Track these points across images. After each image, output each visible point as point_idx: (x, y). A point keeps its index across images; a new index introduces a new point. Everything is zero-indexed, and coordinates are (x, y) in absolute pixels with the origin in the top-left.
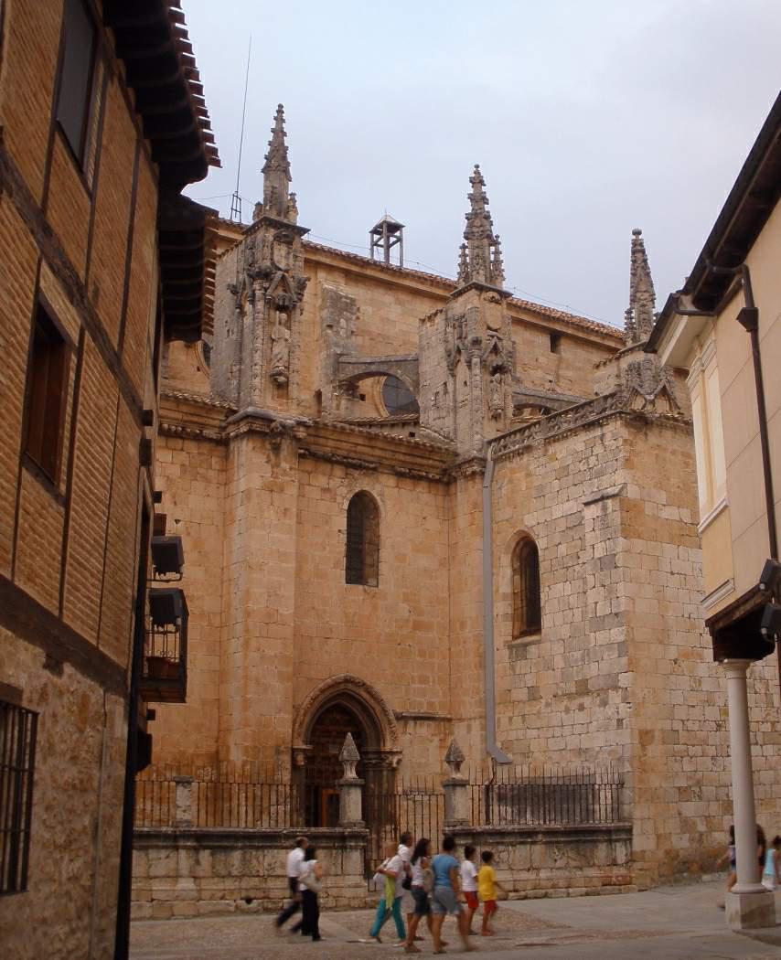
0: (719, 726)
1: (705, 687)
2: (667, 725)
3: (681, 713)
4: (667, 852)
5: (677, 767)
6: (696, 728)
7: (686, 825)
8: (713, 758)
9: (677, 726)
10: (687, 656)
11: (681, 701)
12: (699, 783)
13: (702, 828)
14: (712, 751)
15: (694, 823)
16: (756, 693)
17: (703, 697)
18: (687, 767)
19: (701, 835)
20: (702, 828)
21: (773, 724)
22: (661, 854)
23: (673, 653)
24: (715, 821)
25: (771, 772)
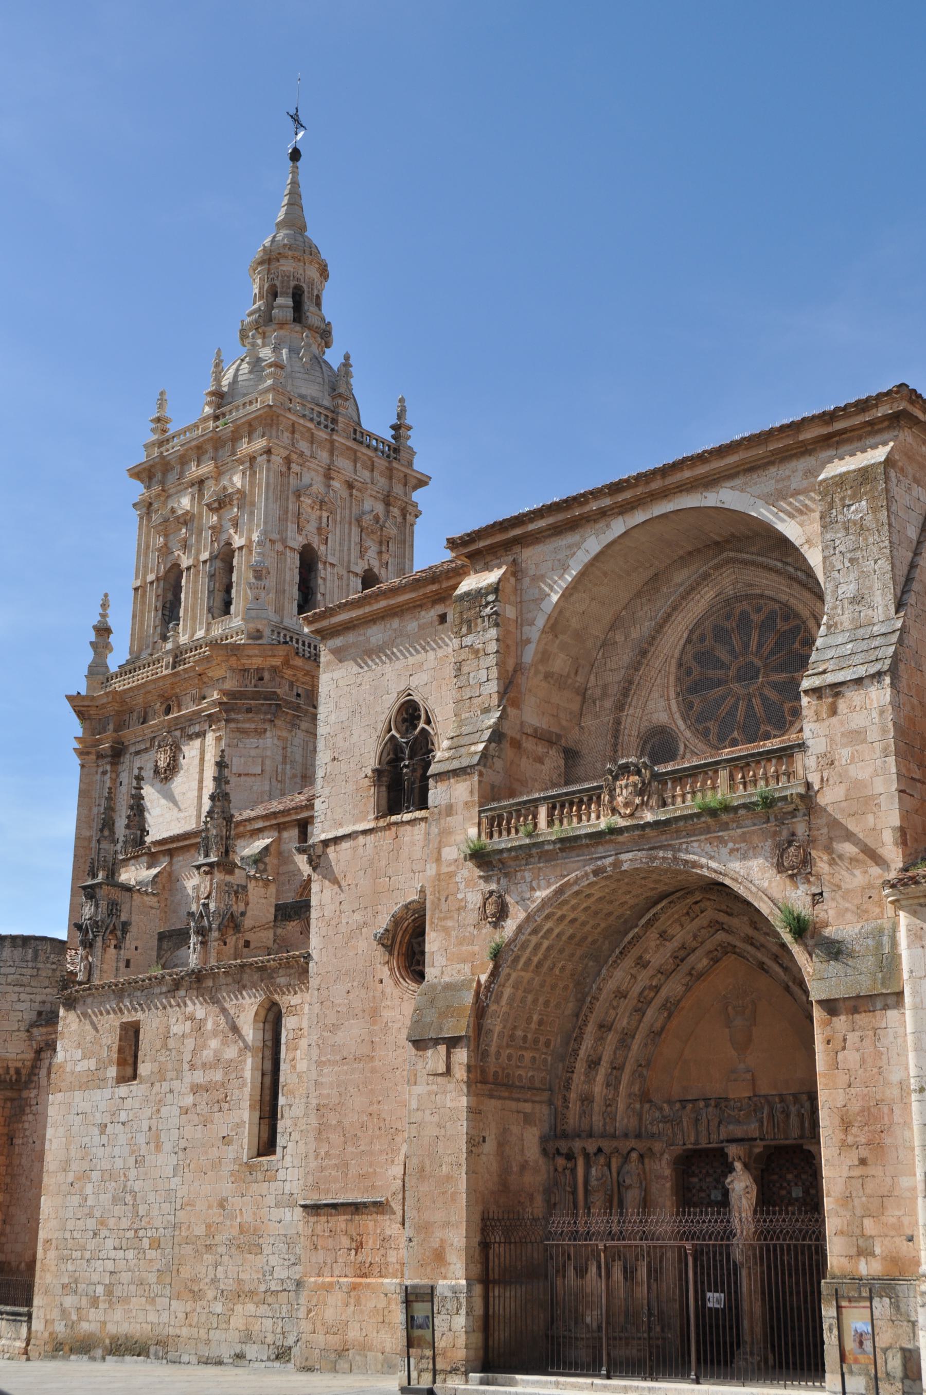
0: (95, 1234)
1: (89, 1203)
2: (59, 1235)
3: (70, 1225)
4: (51, 1334)
5: (63, 1267)
6: (79, 1236)
7: (64, 1312)
8: (88, 1261)
9: (68, 1235)
10: (79, 1179)
11: (71, 1215)
12: (76, 1282)
13: (74, 1317)
14: (88, 1255)
15: (70, 1313)
16: (126, 1204)
17: (86, 1210)
18: (70, 1267)
19: (73, 1323)
20: (74, 1317)
21: (136, 1231)
22: (47, 1334)
23: (71, 1177)
24: (84, 1312)
25: (130, 1273)
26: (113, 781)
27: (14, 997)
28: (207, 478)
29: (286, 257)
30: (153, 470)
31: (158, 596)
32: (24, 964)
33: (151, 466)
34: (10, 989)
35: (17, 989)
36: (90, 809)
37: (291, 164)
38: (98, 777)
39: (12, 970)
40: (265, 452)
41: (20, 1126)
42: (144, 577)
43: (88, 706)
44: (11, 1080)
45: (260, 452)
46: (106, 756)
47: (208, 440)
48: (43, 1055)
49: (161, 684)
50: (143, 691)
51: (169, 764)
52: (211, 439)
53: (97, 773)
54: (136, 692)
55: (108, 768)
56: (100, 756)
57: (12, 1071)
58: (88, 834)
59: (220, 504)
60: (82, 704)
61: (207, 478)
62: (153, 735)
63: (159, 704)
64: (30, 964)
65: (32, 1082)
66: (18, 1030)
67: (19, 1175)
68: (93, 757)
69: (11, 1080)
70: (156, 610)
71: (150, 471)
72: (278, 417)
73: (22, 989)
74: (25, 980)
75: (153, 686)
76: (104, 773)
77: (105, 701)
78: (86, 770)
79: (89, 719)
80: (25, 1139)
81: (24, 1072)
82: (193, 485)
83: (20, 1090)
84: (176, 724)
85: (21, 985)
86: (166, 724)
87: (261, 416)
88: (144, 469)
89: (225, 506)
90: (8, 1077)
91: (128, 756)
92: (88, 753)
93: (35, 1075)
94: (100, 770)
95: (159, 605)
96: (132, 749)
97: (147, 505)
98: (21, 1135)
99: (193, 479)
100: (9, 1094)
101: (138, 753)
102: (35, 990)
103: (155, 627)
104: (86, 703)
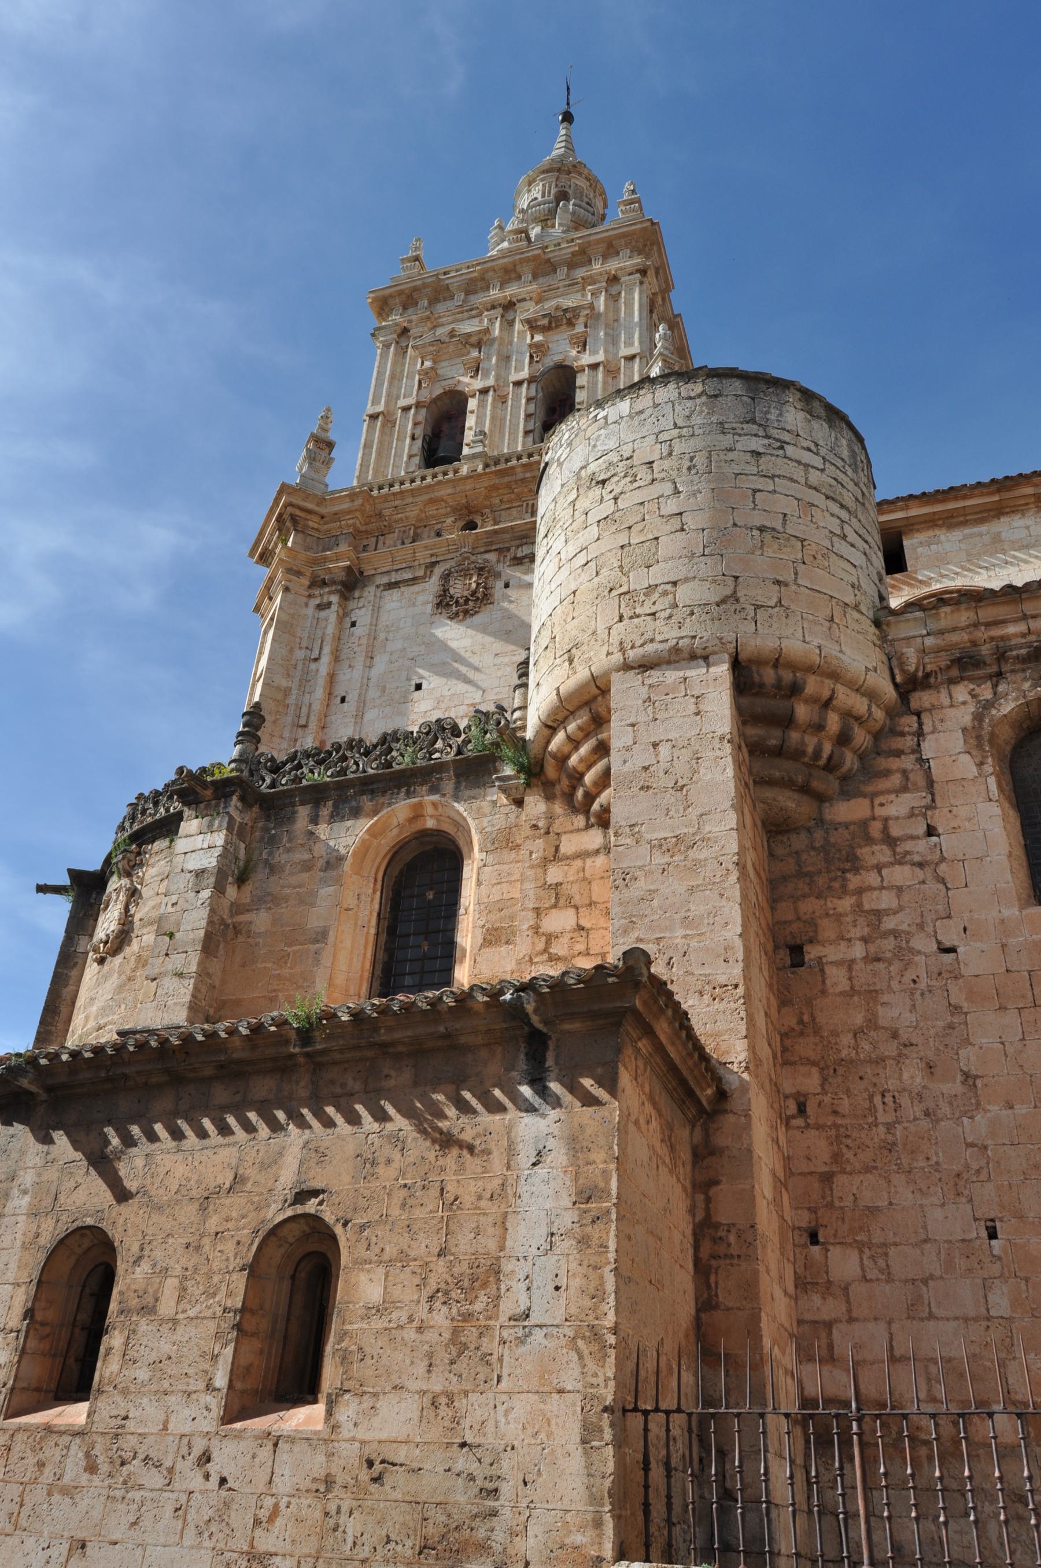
26: (341, 619)
27: (834, 525)
28: (524, 300)
29: (580, 174)
30: (415, 295)
31: (416, 424)
32: (840, 464)
33: (415, 289)
34: (819, 499)
35: (835, 508)
36: (291, 651)
37: (571, 110)
38: (310, 611)
39: (817, 462)
40: (638, 271)
41: (846, 904)
42: (392, 398)
43: (309, 512)
44: (817, 754)
45: (629, 270)
46: (334, 582)
47: (527, 260)
48: (921, 699)
49: (468, 487)
50: (425, 497)
51: (473, 593)
52: (536, 257)
53: (307, 605)
54: (410, 500)
55: (334, 599)
56: (318, 583)
57: (833, 722)
58: (284, 683)
59: (550, 323)
60: (302, 503)
61: (524, 300)
62: (434, 559)
63: (453, 519)
64: (850, 472)
65: (887, 773)
66: (856, 607)
67: (881, 1061)
68: (305, 582)
69: (817, 754)
70: (413, 438)
71: (410, 297)
72: (652, 244)
73: (844, 515)
74: (848, 500)
75: (450, 491)
76: (320, 607)
77: (345, 506)
78: (290, 596)
79: (303, 532)
80: (888, 945)
81: (861, 737)
82: (493, 307)
83: (821, 798)
84: (491, 543)
85: (842, 506)
86: (471, 540)
87: (633, 233)
88: (400, 293)
89: (557, 327)
90: (811, 742)
91: (372, 589)
92: (298, 573)
93: (898, 753)
94: (318, 601)
95: (419, 432)
96: (385, 580)
97: (399, 331)
98: (856, 933)
99: (496, 300)
100: (789, 802)
101: (392, 586)
102: (870, 539)
103: (410, 457)
104: (310, 506)
